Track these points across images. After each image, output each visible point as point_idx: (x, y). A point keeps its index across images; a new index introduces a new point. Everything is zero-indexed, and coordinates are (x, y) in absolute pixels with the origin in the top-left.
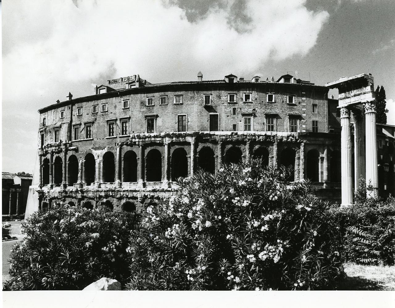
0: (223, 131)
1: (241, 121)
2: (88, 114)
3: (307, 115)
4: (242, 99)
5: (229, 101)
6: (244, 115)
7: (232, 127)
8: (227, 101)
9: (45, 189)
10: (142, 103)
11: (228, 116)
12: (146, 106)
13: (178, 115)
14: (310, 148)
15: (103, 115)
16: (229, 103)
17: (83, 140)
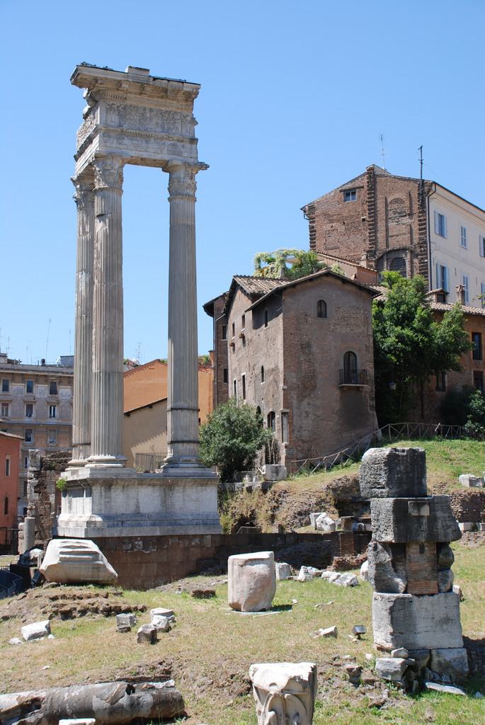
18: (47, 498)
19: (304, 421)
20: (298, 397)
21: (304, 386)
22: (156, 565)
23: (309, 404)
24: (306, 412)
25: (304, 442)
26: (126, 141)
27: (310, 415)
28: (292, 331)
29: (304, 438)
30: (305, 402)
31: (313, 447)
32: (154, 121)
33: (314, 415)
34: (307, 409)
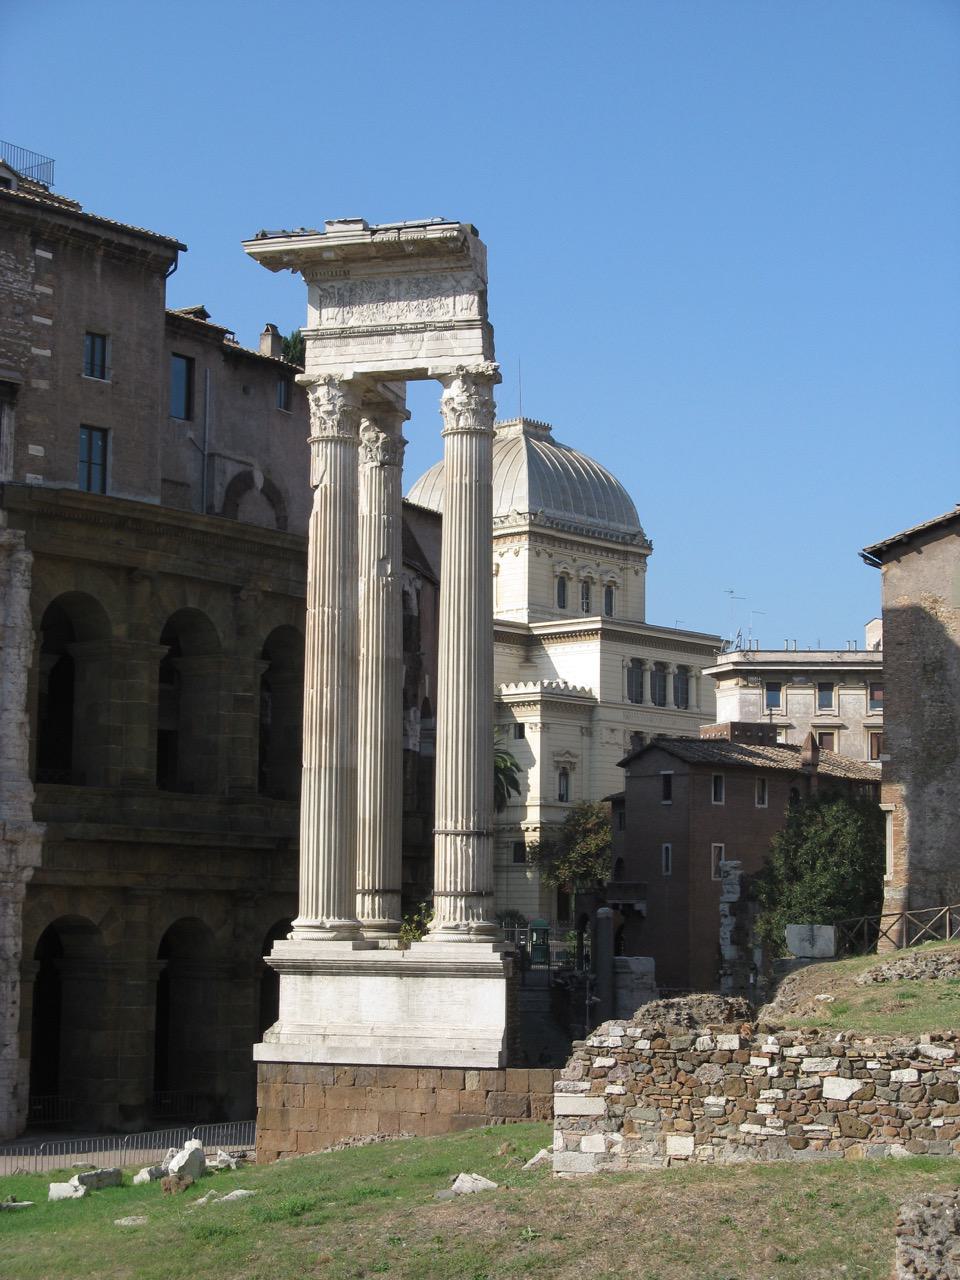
14: (62, 584)
18: (749, 953)
19: (928, 828)
20: (914, 777)
21: (929, 754)
22: (376, 1117)
23: (940, 792)
24: (934, 810)
25: (928, 872)
26: (353, 347)
27: (943, 816)
28: (900, 638)
29: (928, 866)
30: (932, 788)
31: (949, 883)
33: (951, 814)
34: (936, 803)
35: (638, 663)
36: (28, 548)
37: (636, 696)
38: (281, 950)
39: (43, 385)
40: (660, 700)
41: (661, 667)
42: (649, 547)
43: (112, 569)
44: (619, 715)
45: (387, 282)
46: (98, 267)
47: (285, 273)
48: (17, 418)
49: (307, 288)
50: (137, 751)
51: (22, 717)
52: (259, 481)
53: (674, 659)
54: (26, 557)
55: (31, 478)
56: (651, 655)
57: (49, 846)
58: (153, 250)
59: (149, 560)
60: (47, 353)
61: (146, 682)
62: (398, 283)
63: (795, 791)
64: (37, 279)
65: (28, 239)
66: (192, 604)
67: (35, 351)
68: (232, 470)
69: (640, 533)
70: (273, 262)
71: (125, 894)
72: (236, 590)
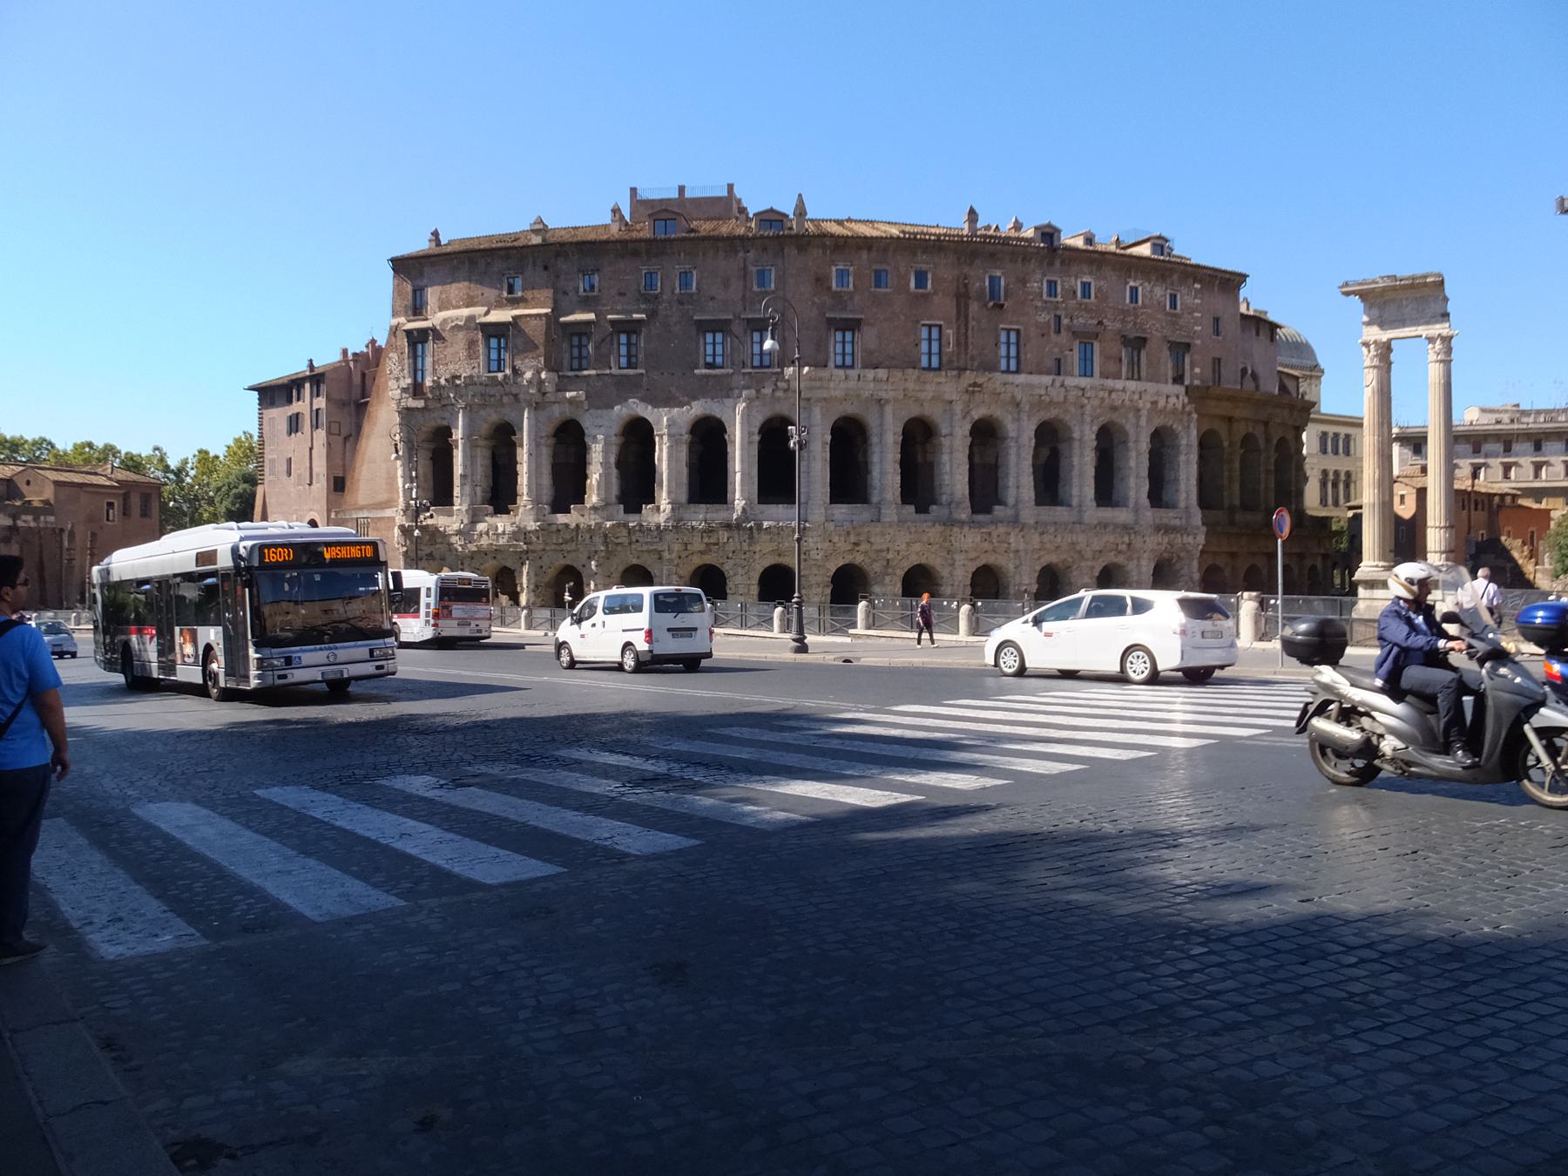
0: (1031, 373)
1: (1071, 350)
2: (621, 294)
3: (1202, 342)
4: (1075, 292)
5: (1045, 296)
6: (1075, 334)
7: (1050, 363)
8: (1041, 296)
9: (443, 521)
10: (818, 280)
11: (1043, 335)
12: (829, 288)
13: (923, 322)
15: (681, 302)
16: (1046, 302)
17: (608, 372)
32: (1410, 307)
35: (1325, 434)
36: (1196, 412)
37: (1324, 451)
38: (1358, 575)
39: (1198, 342)
40: (1336, 452)
41: (1336, 435)
42: (1323, 372)
43: (1222, 418)
44: (1315, 460)
45: (1401, 300)
46: (1216, 289)
47: (1352, 296)
48: (1191, 356)
49: (1362, 305)
50: (1233, 495)
51: (1195, 483)
52: (1250, 372)
53: (1343, 431)
54: (1195, 416)
55: (1197, 382)
56: (1331, 429)
57: (1207, 534)
58: (1237, 279)
59: (1238, 413)
60: (1200, 328)
61: (1237, 465)
62: (1407, 299)
63: (1463, 500)
64: (1195, 297)
65: (1192, 280)
66: (1250, 430)
67: (1196, 328)
68: (1241, 366)
69: (1317, 366)
70: (1347, 294)
71: (1233, 555)
72: (1266, 424)
